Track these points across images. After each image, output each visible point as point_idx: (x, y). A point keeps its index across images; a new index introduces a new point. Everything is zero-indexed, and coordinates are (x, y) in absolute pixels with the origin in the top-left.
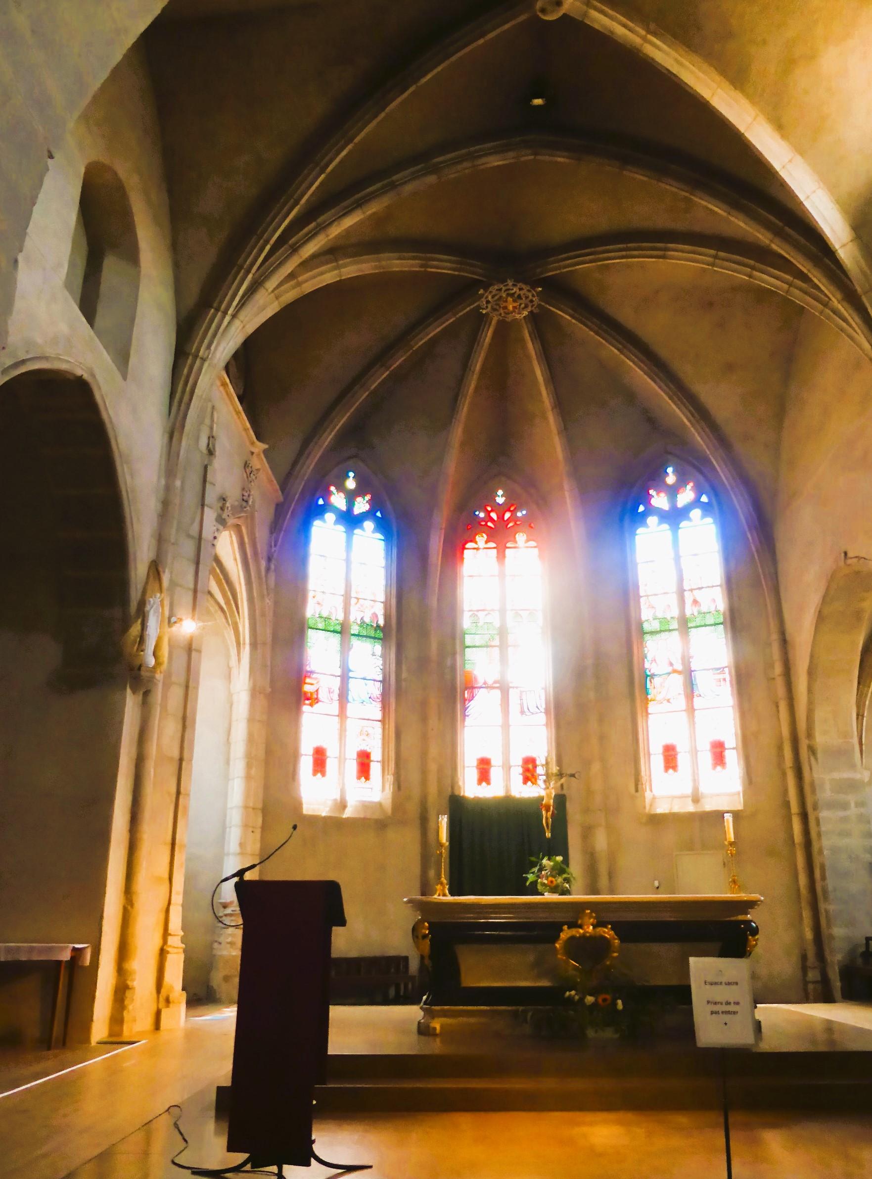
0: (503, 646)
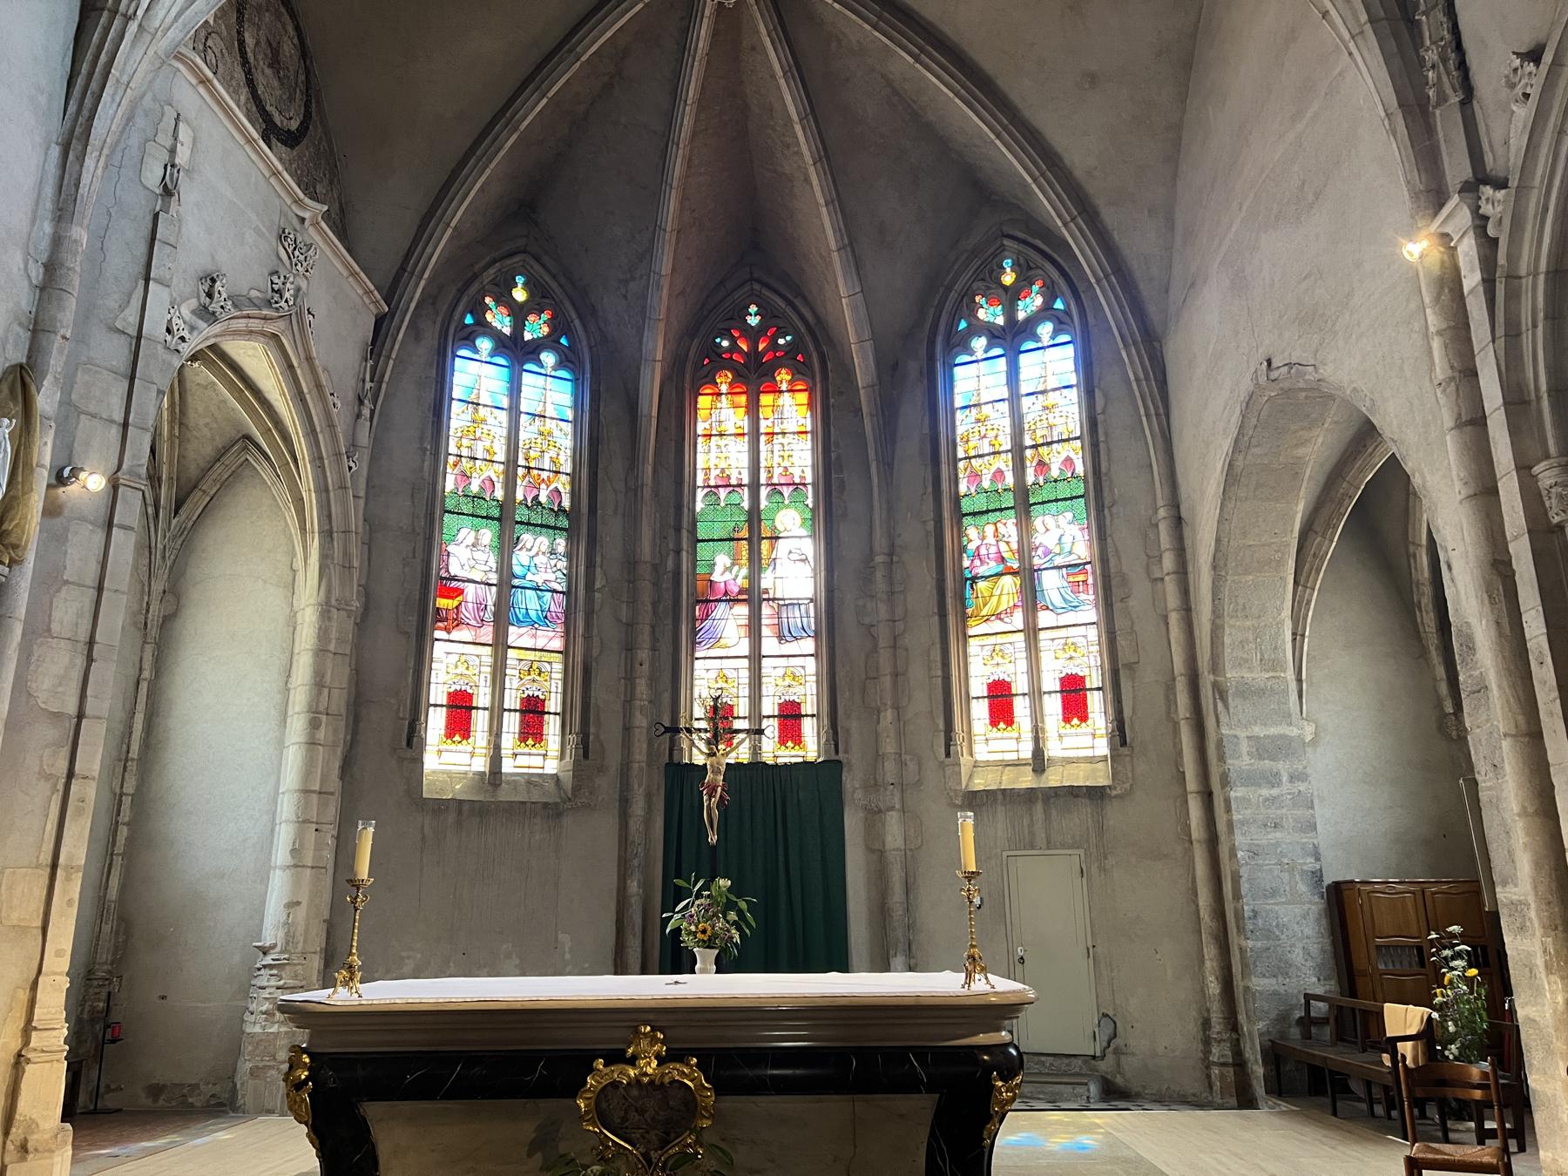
0: (754, 540)
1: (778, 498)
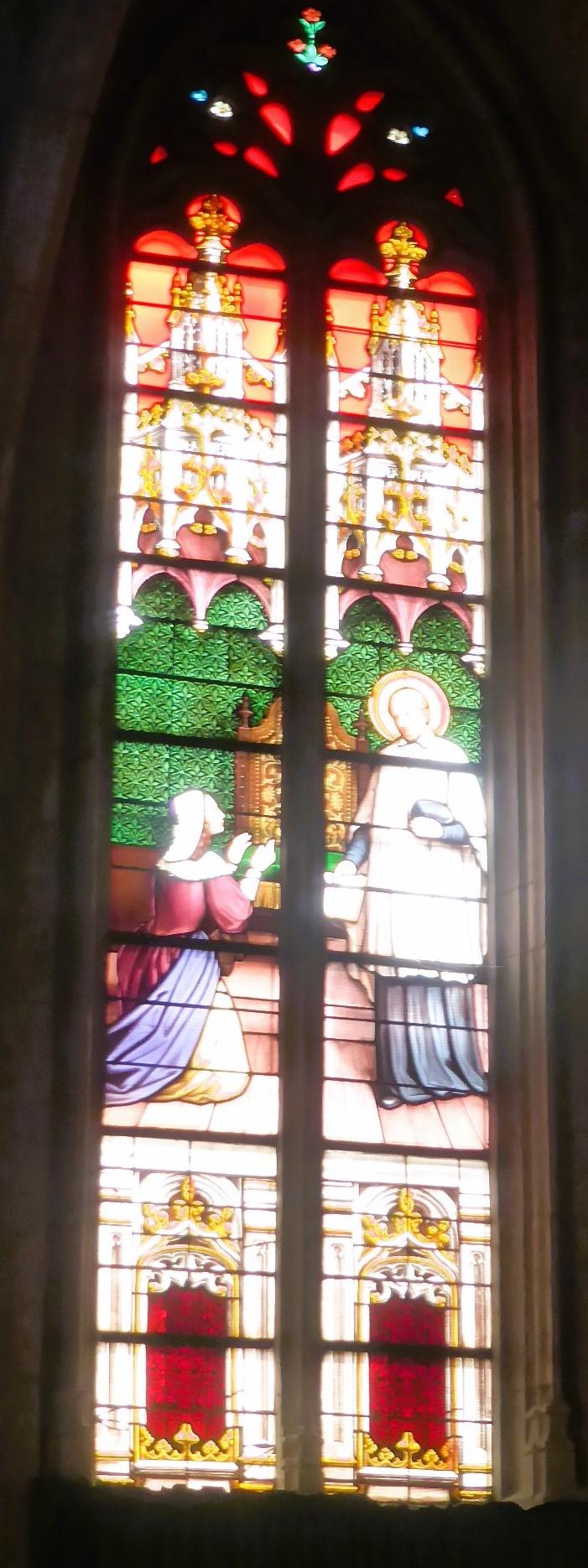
1: (375, 631)
